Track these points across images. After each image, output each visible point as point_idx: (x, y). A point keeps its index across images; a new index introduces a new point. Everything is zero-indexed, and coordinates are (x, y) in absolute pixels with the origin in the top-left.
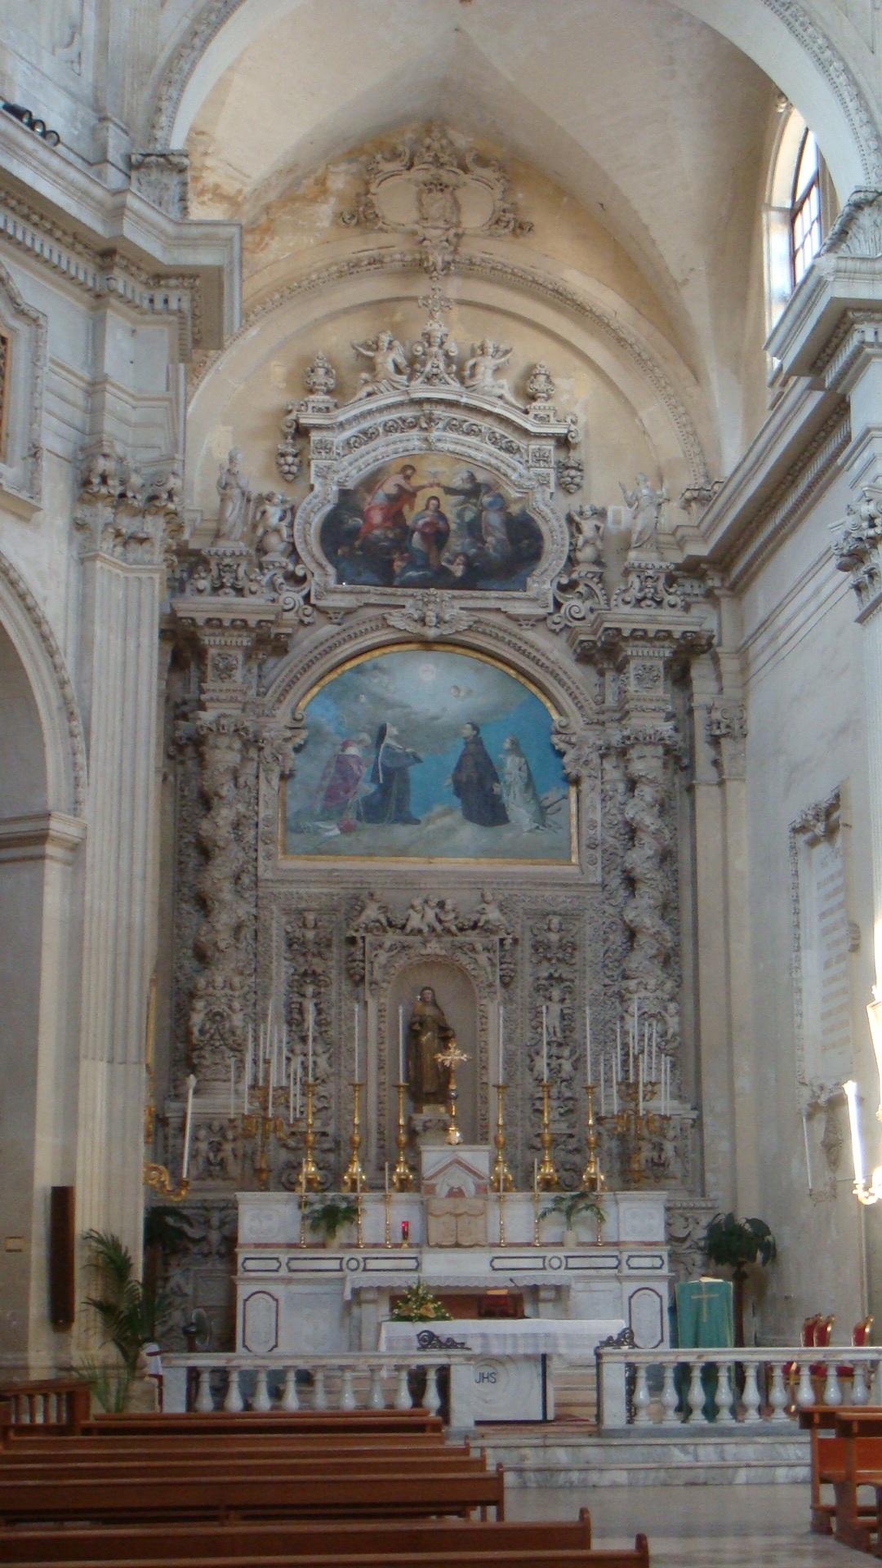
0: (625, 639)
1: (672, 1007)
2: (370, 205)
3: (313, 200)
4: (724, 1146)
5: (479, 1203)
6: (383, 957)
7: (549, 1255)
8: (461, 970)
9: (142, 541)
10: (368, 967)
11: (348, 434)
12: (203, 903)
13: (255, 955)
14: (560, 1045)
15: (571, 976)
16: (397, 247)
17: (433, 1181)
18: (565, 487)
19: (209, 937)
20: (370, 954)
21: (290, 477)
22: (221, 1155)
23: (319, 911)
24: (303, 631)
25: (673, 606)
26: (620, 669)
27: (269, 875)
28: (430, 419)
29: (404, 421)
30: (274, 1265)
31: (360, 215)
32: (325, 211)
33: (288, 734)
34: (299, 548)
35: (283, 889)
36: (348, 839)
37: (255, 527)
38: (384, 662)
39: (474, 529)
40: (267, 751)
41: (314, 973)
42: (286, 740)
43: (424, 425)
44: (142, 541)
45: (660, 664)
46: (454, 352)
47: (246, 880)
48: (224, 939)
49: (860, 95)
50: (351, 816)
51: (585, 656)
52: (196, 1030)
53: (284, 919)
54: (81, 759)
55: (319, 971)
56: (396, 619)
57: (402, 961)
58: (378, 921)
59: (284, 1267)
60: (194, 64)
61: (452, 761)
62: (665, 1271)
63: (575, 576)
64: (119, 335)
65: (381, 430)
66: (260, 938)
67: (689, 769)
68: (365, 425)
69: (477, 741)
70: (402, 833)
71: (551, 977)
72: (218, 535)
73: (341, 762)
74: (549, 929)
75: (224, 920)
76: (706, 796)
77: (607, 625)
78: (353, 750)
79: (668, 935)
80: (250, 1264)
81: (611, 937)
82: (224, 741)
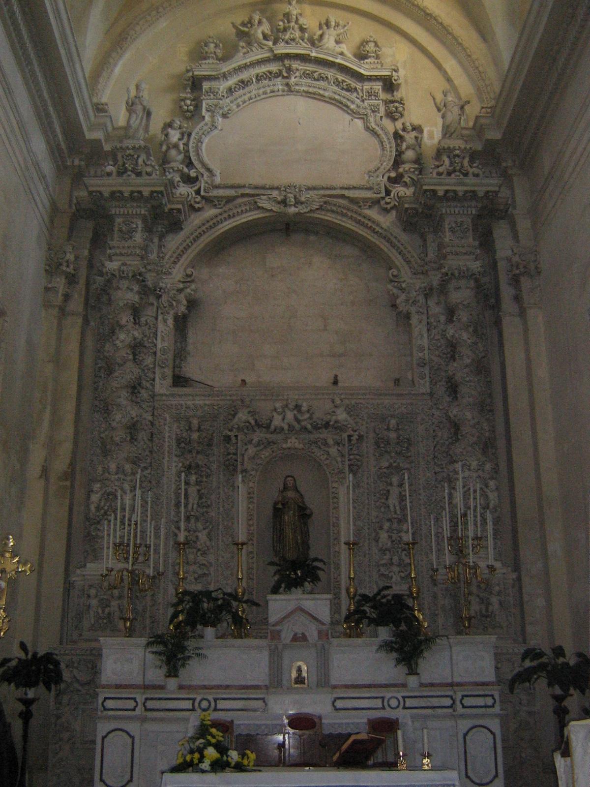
0: (441, 199)
1: (492, 483)
4: (541, 602)
7: (388, 695)
11: (231, 82)
12: (106, 409)
13: (151, 452)
17: (278, 628)
18: (391, 116)
21: (189, 114)
25: (477, 175)
26: (437, 228)
28: (289, 69)
29: (270, 73)
30: (132, 704)
33: (181, 286)
34: (194, 159)
37: (161, 145)
40: (164, 298)
41: (198, 466)
42: (180, 291)
43: (285, 75)
45: (468, 221)
47: (144, 394)
52: (93, 508)
55: (200, 463)
57: (266, 454)
58: (248, 422)
59: (140, 708)
62: (497, 709)
63: (401, 170)
65: (254, 80)
66: (155, 439)
67: (496, 307)
71: (390, 466)
72: (127, 137)
74: (388, 429)
77: (425, 187)
79: (485, 425)
80: (110, 704)
81: (440, 434)
82: (124, 284)
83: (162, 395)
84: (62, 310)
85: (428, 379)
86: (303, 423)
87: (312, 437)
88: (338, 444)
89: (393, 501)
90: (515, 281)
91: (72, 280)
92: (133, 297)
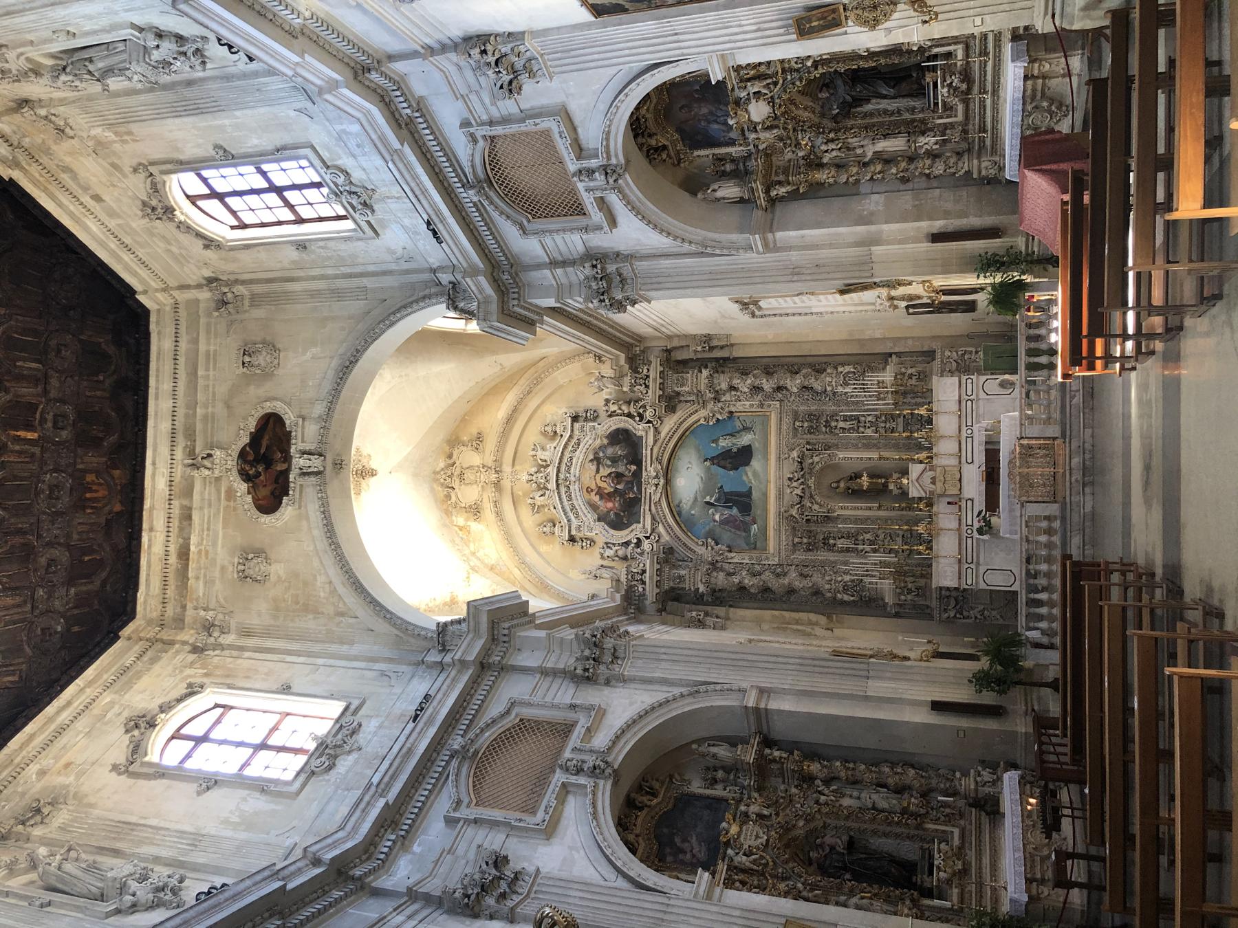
1: (840, 369)
2: (470, 507)
3: (469, 532)
8: (822, 469)
9: (615, 650)
11: (572, 518)
12: (791, 591)
16: (489, 494)
23: (795, 536)
24: (662, 540)
26: (678, 394)
30: (969, 571)
31: (475, 511)
32: (474, 526)
35: (783, 554)
36: (759, 521)
38: (676, 502)
39: (614, 460)
44: (615, 650)
46: (534, 469)
47: (779, 570)
48: (806, 583)
49: (405, 307)
50: (747, 518)
51: (671, 409)
54: (718, 687)
56: (656, 498)
57: (818, 498)
60: (399, 618)
61: (721, 470)
64: (520, 658)
67: (725, 359)
68: (568, 510)
69: (712, 459)
70: (755, 495)
72: (618, 581)
73: (723, 522)
76: (737, 353)
78: (717, 517)
79: (804, 371)
80: (969, 582)
84: (728, 619)
89: (846, 425)
90: (712, 348)
91: (707, 614)
92: (721, 575)
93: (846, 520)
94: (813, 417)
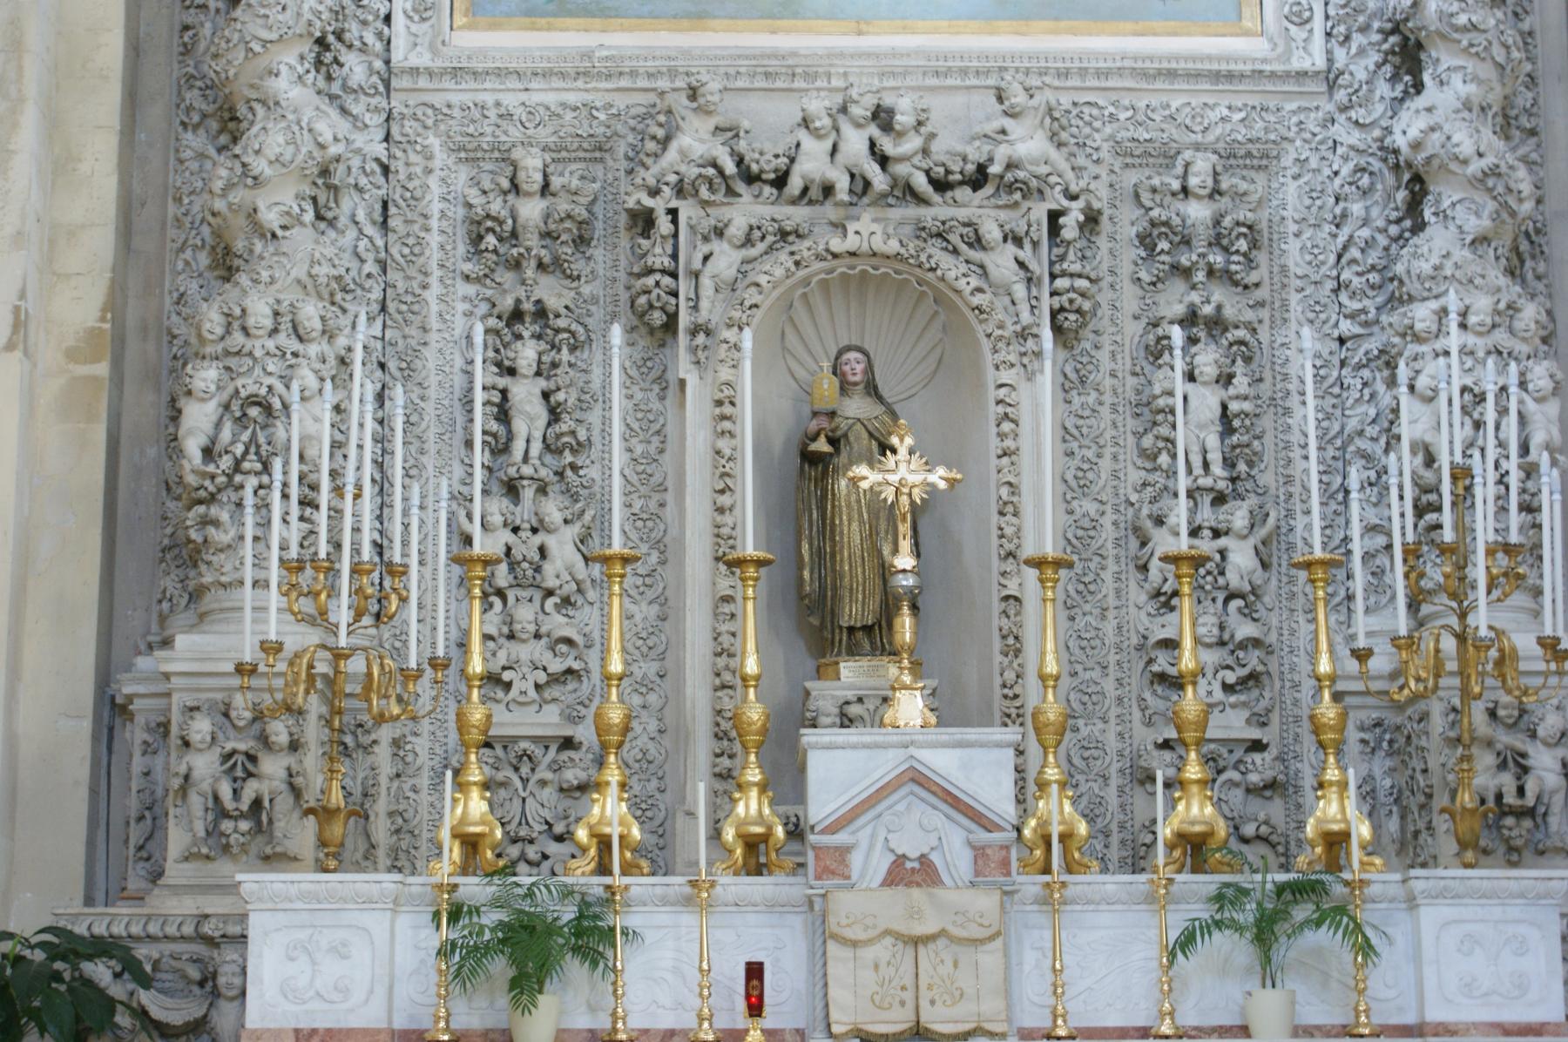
5: (985, 902)
6: (726, 260)
8: (943, 299)
10: (684, 287)
12: (229, 123)
14: (1219, 499)
15: (1249, 315)
17: (841, 838)
19: (236, 196)
20: (690, 255)
22: (250, 790)
23: (558, 153)
27: (421, 59)
35: (458, 95)
41: (541, 313)
47: (356, 68)
48: (278, 201)
52: (193, 447)
53: (462, 175)
55: (553, 303)
58: (715, 165)
74: (1185, 190)
75: (269, 142)
79: (1523, 180)
81: (1357, 208)
83: (415, 72)
85: (1318, 24)
86: (901, 169)
87: (928, 215)
88: (1018, 241)
93: (654, 437)
94: (1240, 246)
